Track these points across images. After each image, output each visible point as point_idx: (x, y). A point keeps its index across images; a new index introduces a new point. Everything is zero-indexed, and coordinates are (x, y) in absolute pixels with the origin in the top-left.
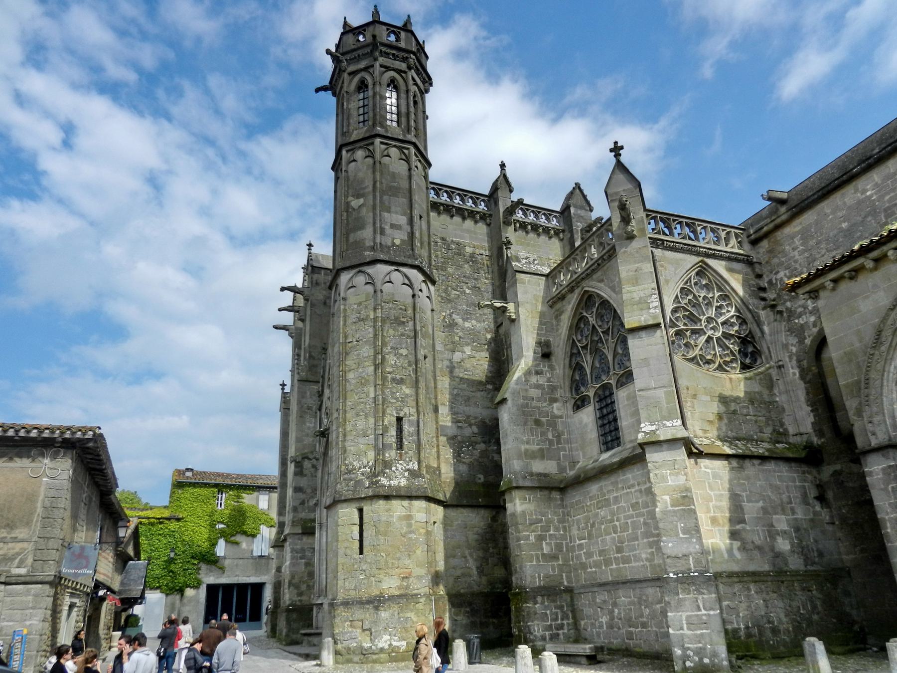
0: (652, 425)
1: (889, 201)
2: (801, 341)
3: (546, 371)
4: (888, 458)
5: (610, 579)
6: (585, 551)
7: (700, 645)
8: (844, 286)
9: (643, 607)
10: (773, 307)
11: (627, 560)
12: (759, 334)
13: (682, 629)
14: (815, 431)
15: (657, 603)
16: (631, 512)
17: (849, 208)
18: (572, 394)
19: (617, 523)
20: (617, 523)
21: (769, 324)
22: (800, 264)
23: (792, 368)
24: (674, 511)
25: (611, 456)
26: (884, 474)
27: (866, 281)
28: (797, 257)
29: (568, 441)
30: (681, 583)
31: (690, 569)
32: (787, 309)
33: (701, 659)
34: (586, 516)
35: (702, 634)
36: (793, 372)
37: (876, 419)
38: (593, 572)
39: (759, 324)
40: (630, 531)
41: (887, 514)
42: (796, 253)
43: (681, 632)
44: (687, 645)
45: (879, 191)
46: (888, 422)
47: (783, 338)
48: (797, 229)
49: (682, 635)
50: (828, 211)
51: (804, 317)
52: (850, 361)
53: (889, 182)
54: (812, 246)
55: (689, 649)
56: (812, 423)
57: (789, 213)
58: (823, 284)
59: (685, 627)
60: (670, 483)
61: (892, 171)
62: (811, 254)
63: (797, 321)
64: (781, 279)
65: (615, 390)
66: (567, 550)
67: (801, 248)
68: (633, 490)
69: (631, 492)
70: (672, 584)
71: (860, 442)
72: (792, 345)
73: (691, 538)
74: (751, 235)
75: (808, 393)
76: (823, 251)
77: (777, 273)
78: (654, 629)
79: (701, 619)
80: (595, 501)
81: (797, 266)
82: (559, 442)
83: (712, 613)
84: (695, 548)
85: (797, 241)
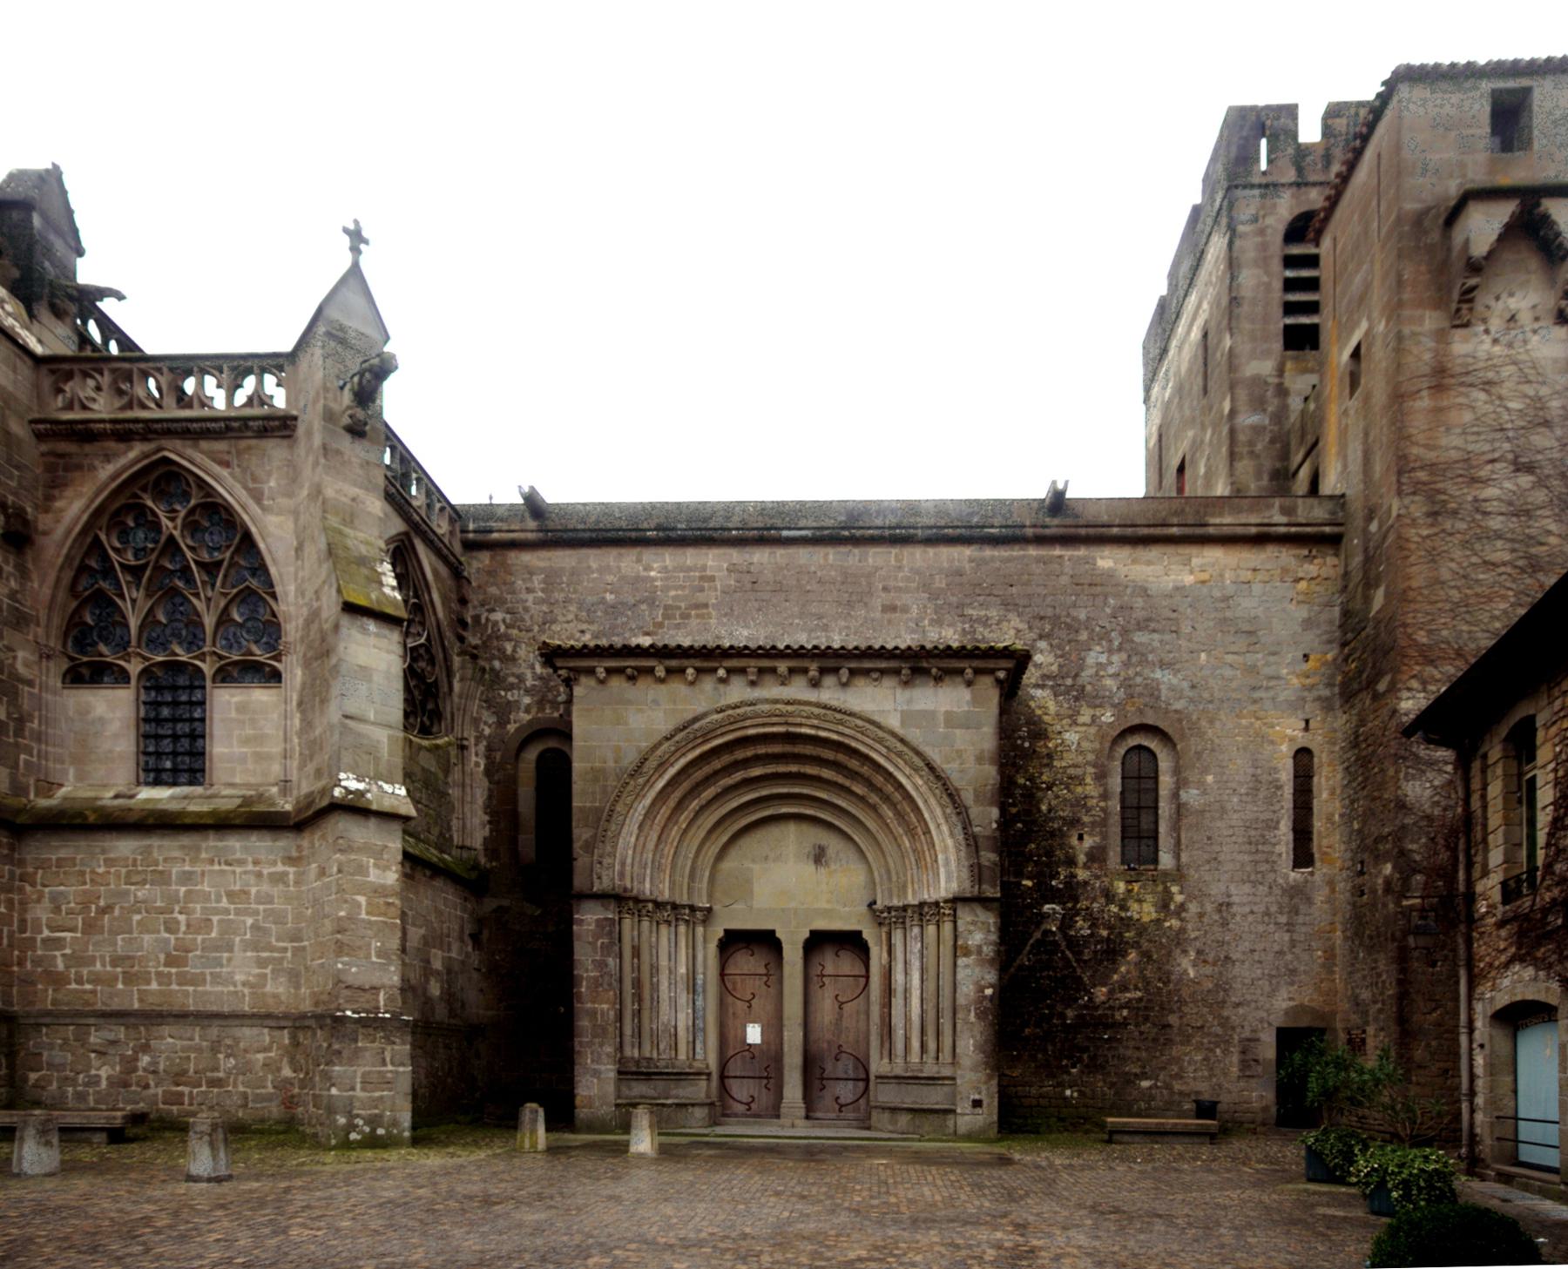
0: (359, 781)
1: (675, 598)
2: (502, 722)
3: (10, 574)
4: (607, 909)
5: (136, 1006)
6: (68, 951)
7: (377, 1111)
8: (617, 683)
9: (221, 1056)
10: (474, 657)
11: (197, 980)
12: (446, 689)
13: (353, 1089)
14: (486, 850)
15: (259, 1052)
16: (224, 903)
17: (623, 578)
18: (64, 645)
19: (182, 918)
20: (182, 918)
21: (462, 680)
22: (531, 617)
23: (477, 755)
24: (370, 922)
25: (172, 798)
26: (597, 926)
27: (646, 690)
28: (529, 604)
29: (39, 737)
30: (363, 1027)
31: (378, 1008)
32: (492, 669)
33: (373, 1130)
34: (85, 892)
35: (382, 1097)
36: (476, 761)
37: (606, 861)
38: (85, 992)
39: (450, 674)
40: (213, 935)
41: (587, 971)
42: (530, 597)
43: (351, 1093)
44: (355, 1112)
45: (667, 579)
46: (617, 867)
47: (475, 707)
48: (542, 564)
49: (351, 1098)
50: (594, 566)
51: (515, 692)
52: (596, 780)
53: (681, 575)
54: (557, 601)
55: (358, 1116)
56: (485, 839)
57: (541, 535)
58: (595, 667)
59: (358, 1086)
60: (372, 878)
61: (688, 562)
62: (552, 612)
63: (503, 693)
64: (495, 623)
65: (208, 683)
66: (11, 945)
67: (540, 594)
68: (238, 870)
69: (234, 872)
70: (350, 1026)
71: (579, 882)
72: (485, 723)
73: (389, 964)
74: (468, 532)
75: (490, 797)
76: (571, 617)
77: (492, 610)
78: (241, 1089)
79: (384, 1077)
80: (124, 870)
81: (527, 617)
82: (19, 732)
83: (401, 1069)
84: (391, 979)
85: (537, 583)
